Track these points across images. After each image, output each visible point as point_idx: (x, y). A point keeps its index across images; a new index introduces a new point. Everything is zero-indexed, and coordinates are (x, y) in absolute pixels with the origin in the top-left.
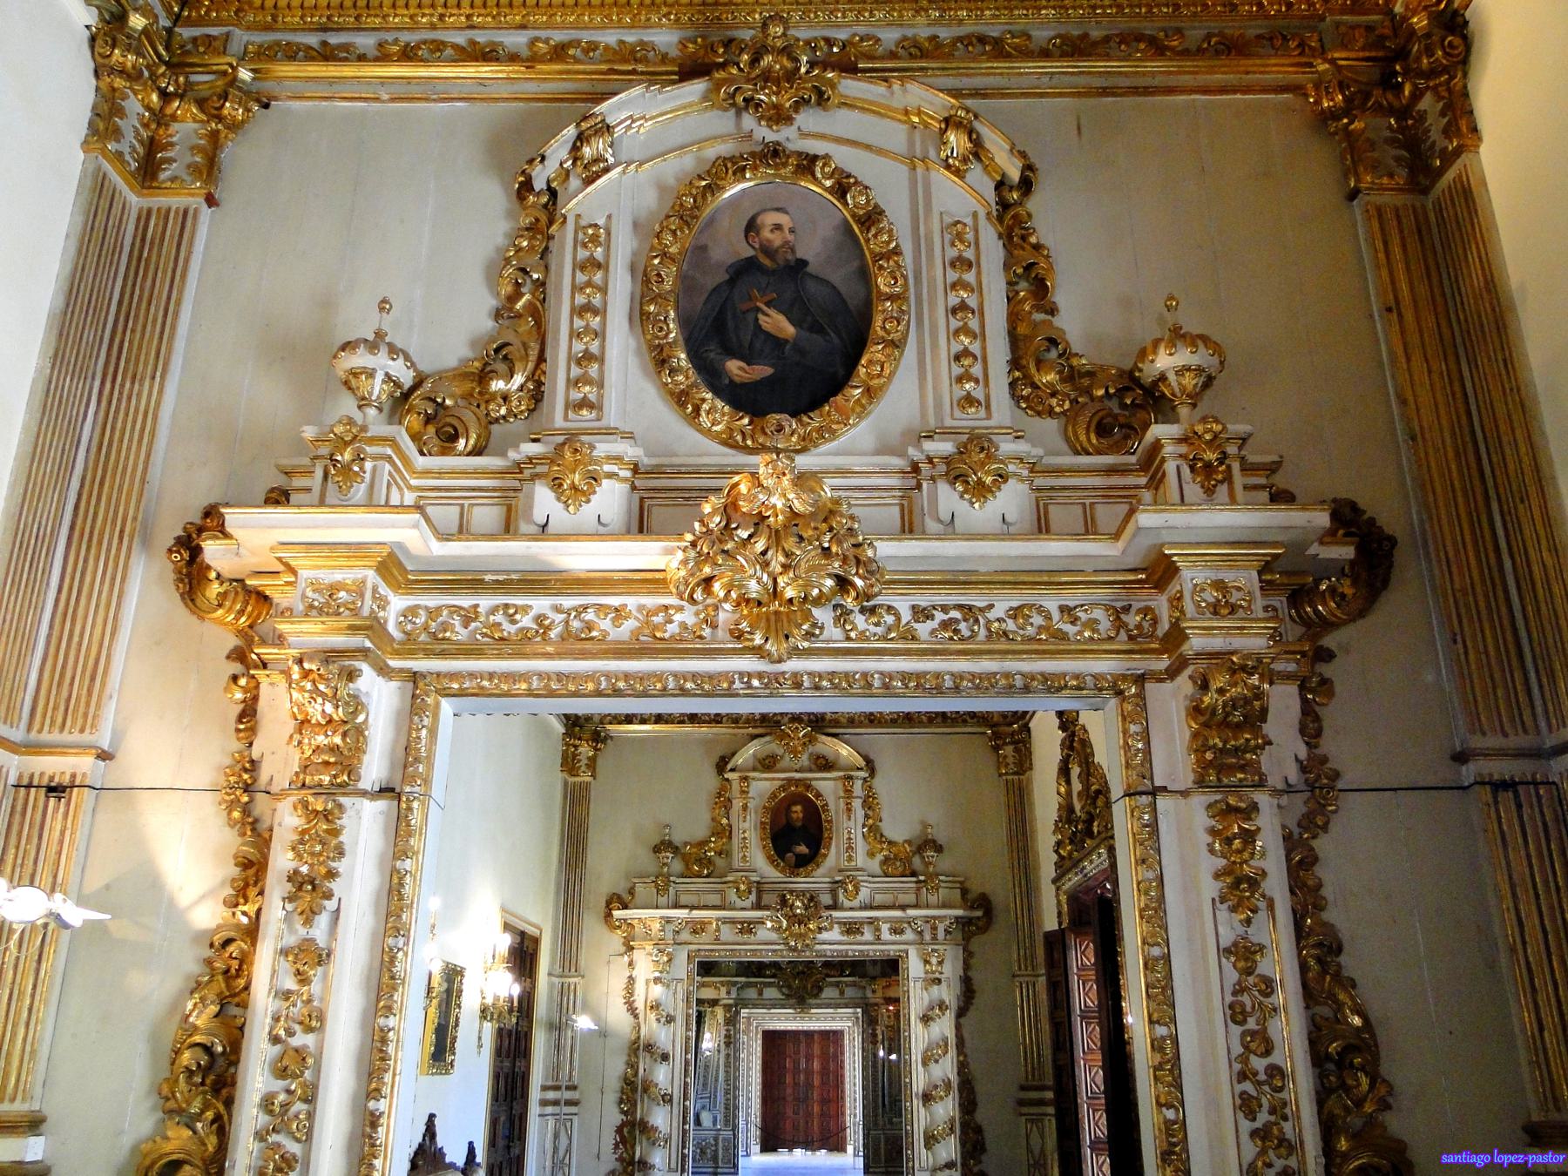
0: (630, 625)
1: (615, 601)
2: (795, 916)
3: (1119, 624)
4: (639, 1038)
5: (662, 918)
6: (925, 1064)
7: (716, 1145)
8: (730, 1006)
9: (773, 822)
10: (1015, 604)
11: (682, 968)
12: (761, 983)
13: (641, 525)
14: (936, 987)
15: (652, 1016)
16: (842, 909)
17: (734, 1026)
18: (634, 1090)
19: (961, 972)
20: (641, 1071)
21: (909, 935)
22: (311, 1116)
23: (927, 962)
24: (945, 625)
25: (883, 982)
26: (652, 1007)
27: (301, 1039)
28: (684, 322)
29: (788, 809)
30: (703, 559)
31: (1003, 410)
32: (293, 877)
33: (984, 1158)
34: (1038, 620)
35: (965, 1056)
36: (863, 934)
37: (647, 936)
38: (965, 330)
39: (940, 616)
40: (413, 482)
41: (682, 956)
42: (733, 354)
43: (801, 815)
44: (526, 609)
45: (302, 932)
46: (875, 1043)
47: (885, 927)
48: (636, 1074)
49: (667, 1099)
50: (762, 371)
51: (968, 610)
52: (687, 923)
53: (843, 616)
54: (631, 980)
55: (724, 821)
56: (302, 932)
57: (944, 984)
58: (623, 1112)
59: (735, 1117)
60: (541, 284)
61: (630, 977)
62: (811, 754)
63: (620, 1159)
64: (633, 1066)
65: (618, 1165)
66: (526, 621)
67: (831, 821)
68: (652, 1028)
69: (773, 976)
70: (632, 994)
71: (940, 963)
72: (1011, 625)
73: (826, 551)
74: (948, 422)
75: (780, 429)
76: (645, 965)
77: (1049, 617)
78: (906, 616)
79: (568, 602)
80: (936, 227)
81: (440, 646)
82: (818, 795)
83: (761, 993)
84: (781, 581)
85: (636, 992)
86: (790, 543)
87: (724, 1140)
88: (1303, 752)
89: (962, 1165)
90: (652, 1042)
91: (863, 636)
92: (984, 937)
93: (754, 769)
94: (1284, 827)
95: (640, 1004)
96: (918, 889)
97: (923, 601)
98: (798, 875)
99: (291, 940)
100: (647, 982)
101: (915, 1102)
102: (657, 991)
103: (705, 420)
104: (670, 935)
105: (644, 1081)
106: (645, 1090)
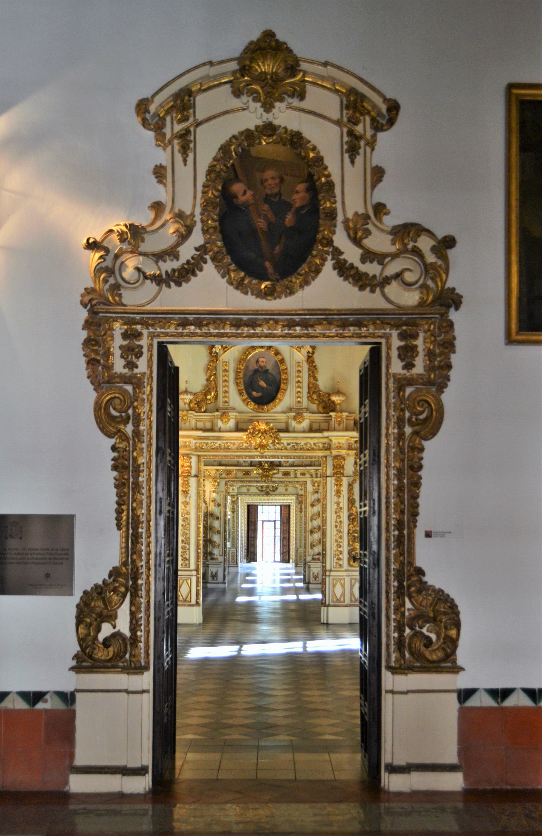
0: (236, 446)
1: (233, 442)
2: (265, 469)
3: (324, 447)
5: (215, 469)
6: (311, 521)
8: (234, 495)
10: (305, 442)
11: (222, 487)
12: (248, 486)
13: (238, 429)
15: (212, 504)
16: (283, 466)
17: (236, 504)
21: (308, 475)
22: (190, 527)
23: (313, 486)
24: (293, 446)
27: (186, 516)
28: (245, 383)
30: (249, 438)
31: (305, 402)
32: (183, 491)
34: (309, 446)
36: (290, 475)
37: (209, 476)
38: (299, 387)
39: (292, 445)
40: (194, 417)
41: (223, 482)
42: (254, 390)
44: (217, 443)
45: (185, 500)
47: (298, 473)
48: (207, 523)
49: (219, 532)
50: (260, 394)
51: (296, 443)
53: (274, 445)
56: (185, 500)
57: (319, 493)
59: (237, 543)
60: (215, 374)
64: (205, 521)
66: (217, 445)
68: (212, 508)
71: (319, 486)
72: (304, 446)
73: (271, 436)
74: (295, 407)
75: (263, 409)
76: (209, 486)
77: (311, 445)
78: (286, 445)
79: (225, 442)
80: (294, 363)
81: (202, 449)
83: (248, 490)
84: (263, 441)
85: (206, 496)
86: (265, 435)
87: (232, 553)
88: (353, 469)
91: (278, 449)
94: (348, 482)
95: (207, 500)
97: (289, 442)
99: (183, 501)
100: (210, 492)
102: (214, 495)
103: (249, 406)
104: (218, 475)
106: (211, 529)
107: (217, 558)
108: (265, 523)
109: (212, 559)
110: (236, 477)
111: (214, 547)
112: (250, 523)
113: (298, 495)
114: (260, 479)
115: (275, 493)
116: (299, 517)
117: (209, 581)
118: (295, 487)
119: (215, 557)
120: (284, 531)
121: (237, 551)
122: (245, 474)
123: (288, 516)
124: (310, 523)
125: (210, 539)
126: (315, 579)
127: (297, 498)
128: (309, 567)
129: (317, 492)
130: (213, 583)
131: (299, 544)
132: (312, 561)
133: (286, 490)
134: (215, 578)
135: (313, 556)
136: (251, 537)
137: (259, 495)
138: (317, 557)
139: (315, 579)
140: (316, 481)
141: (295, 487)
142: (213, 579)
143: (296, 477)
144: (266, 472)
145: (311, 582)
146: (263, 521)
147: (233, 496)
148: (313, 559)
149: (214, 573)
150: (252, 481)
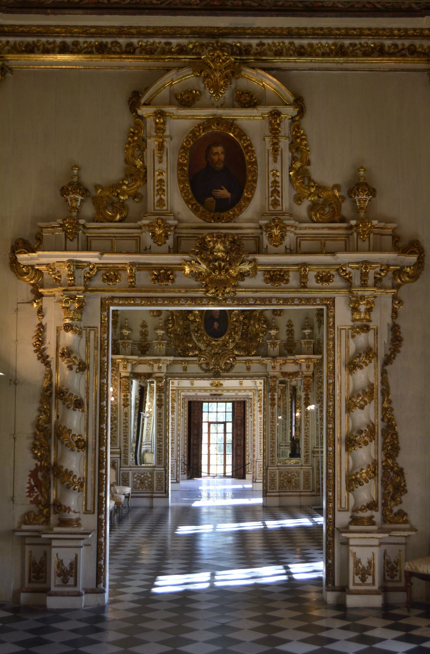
2: (217, 259)
4: (51, 385)
6: (349, 410)
7: (152, 477)
8: (161, 377)
9: (191, 165)
14: (363, 335)
15: (64, 364)
16: (266, 253)
18: (47, 436)
19: (389, 320)
20: (54, 419)
21: (337, 282)
23: (355, 310)
25: (280, 360)
26: (63, 354)
29: (209, 149)
33: (404, 498)
35: (390, 402)
36: (288, 281)
37: (57, 283)
43: (222, 157)
46: (273, 405)
47: (312, 275)
48: (49, 420)
52: (99, 269)
54: (41, 328)
55: (139, 163)
57: (371, 333)
58: (35, 457)
59: (166, 458)
61: (40, 325)
62: (236, 90)
63: (36, 502)
65: (34, 508)
67: (255, 163)
69: (195, 356)
70: (42, 342)
71: (369, 310)
82: (241, 134)
83: (185, 369)
85: (47, 341)
87: (158, 474)
89: (383, 505)
90: (64, 388)
92: (416, 285)
93: (171, 104)
95: (51, 352)
96: (348, 236)
98: (219, 220)
101: (337, 447)
105: (57, 427)
106: (58, 435)
107: (78, 519)
108: (212, 425)
109: (63, 523)
110: (132, 287)
111: (68, 487)
112: (192, 425)
113: (267, 378)
114: (200, 294)
115: (230, 374)
116: (270, 414)
117: (53, 589)
118: (263, 364)
119: (73, 516)
120: (237, 435)
121: (166, 471)
122: (157, 278)
123: (242, 416)
124: (344, 416)
125: (56, 464)
126: (363, 580)
127: (266, 383)
128: (346, 543)
129: (366, 328)
130: (62, 594)
131: (270, 458)
132: (352, 528)
133: (248, 369)
134: (71, 580)
135: (355, 510)
136: (194, 445)
137: (202, 378)
138: (367, 514)
139: (363, 580)
140: (362, 298)
141: (263, 364)
142: (65, 582)
143: (304, 286)
144: (220, 269)
145: (352, 587)
146: (209, 423)
147: (159, 379)
148: (355, 520)
149: (66, 564)
150: (179, 298)
